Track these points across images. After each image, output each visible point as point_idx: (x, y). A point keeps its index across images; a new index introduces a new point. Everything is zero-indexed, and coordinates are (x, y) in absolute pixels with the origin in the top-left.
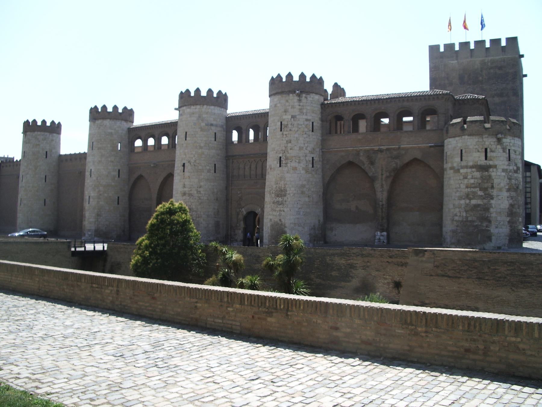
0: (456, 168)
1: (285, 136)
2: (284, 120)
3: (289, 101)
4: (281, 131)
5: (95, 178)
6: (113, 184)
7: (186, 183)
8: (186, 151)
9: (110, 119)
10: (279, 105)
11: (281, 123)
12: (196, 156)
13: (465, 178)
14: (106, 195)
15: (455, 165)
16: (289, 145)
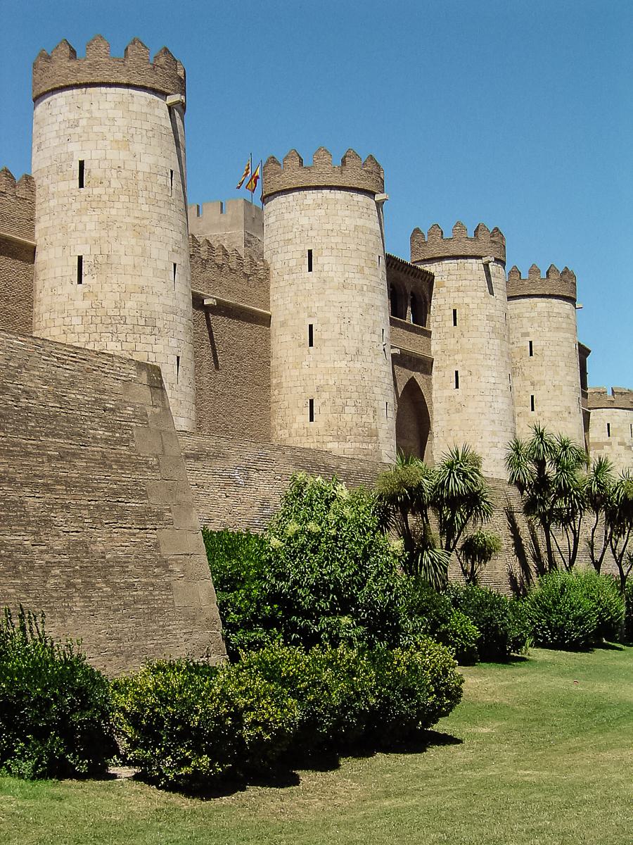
15: (626, 441)
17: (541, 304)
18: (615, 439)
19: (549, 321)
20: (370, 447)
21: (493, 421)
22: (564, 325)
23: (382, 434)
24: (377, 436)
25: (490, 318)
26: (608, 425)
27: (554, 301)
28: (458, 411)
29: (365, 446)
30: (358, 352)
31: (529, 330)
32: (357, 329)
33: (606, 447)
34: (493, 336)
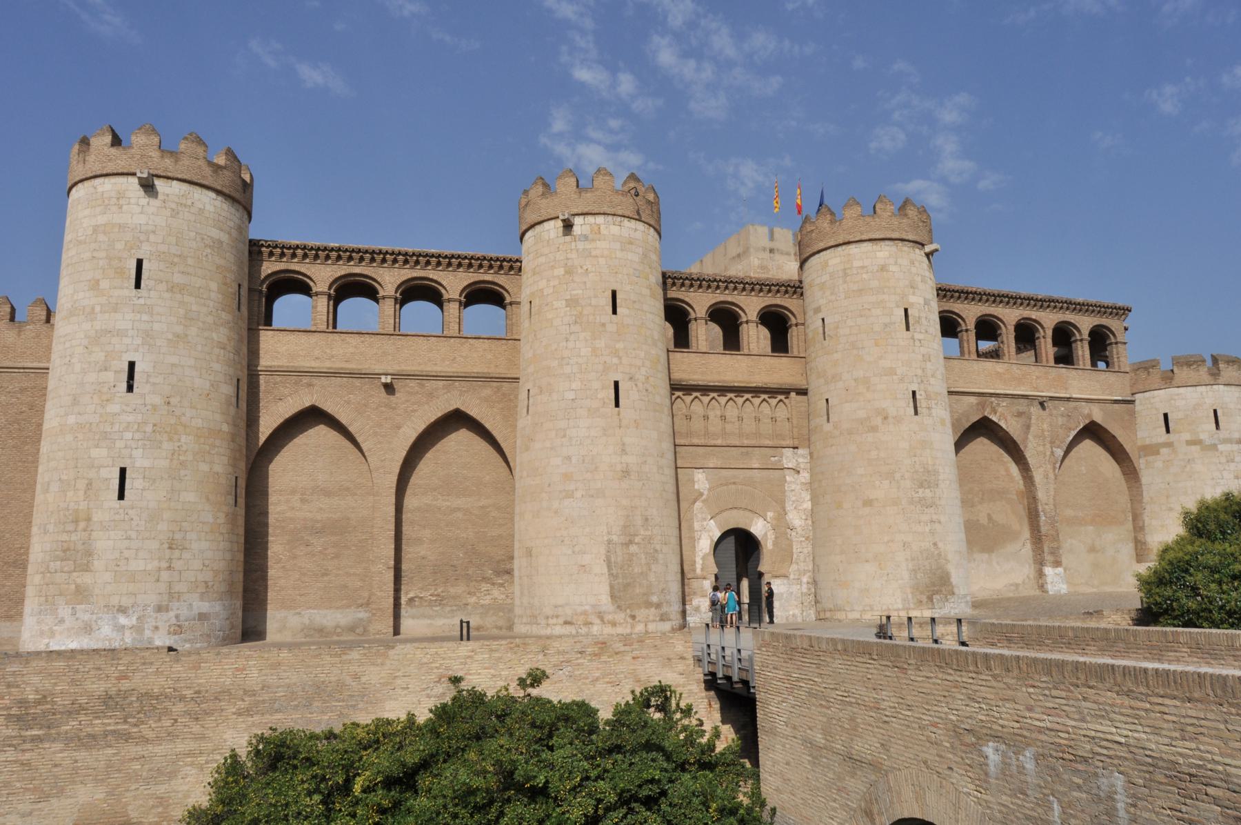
0: (1208, 442)
1: (917, 343)
2: (912, 304)
3: (917, 264)
4: (908, 329)
5: (157, 400)
6: (225, 428)
7: (627, 440)
8: (620, 345)
9: (218, 192)
10: (892, 268)
11: (906, 310)
12: (648, 363)
13: (1233, 461)
14: (204, 467)
15: (1202, 436)
16: (929, 365)
17: (833, 260)
18: (1180, 436)
19: (845, 282)
20: (74, 538)
21: (569, 458)
22: (875, 284)
23: (97, 517)
24: (89, 519)
25: (572, 302)
26: (1166, 416)
27: (853, 249)
28: (527, 449)
29: (65, 537)
30: (75, 401)
31: (822, 302)
32: (78, 367)
33: (1164, 451)
34: (574, 328)
